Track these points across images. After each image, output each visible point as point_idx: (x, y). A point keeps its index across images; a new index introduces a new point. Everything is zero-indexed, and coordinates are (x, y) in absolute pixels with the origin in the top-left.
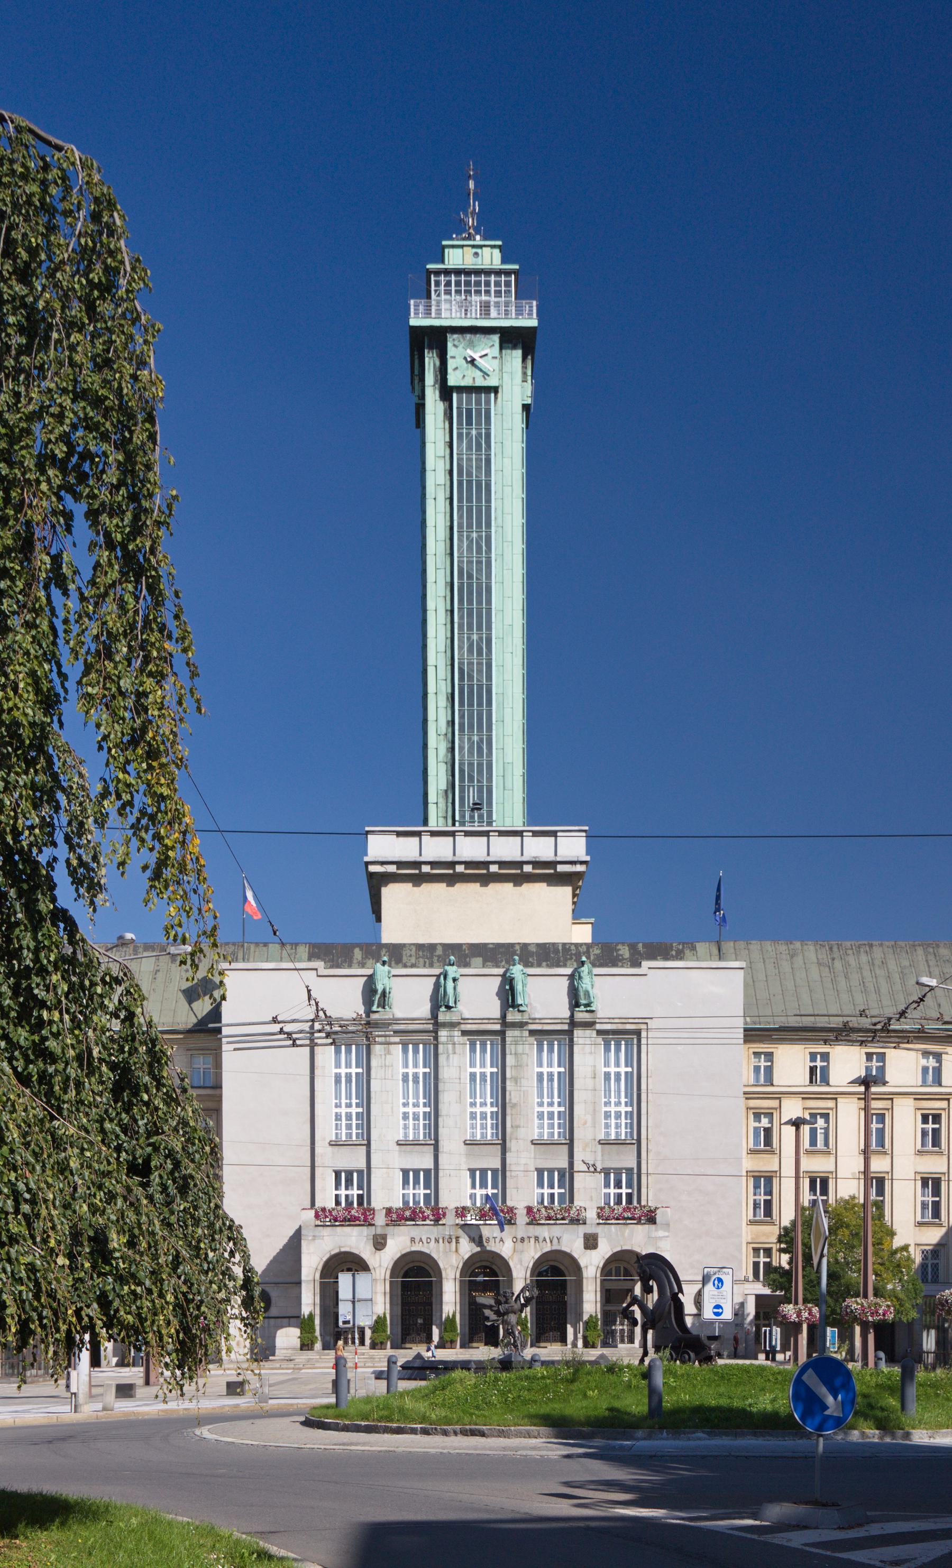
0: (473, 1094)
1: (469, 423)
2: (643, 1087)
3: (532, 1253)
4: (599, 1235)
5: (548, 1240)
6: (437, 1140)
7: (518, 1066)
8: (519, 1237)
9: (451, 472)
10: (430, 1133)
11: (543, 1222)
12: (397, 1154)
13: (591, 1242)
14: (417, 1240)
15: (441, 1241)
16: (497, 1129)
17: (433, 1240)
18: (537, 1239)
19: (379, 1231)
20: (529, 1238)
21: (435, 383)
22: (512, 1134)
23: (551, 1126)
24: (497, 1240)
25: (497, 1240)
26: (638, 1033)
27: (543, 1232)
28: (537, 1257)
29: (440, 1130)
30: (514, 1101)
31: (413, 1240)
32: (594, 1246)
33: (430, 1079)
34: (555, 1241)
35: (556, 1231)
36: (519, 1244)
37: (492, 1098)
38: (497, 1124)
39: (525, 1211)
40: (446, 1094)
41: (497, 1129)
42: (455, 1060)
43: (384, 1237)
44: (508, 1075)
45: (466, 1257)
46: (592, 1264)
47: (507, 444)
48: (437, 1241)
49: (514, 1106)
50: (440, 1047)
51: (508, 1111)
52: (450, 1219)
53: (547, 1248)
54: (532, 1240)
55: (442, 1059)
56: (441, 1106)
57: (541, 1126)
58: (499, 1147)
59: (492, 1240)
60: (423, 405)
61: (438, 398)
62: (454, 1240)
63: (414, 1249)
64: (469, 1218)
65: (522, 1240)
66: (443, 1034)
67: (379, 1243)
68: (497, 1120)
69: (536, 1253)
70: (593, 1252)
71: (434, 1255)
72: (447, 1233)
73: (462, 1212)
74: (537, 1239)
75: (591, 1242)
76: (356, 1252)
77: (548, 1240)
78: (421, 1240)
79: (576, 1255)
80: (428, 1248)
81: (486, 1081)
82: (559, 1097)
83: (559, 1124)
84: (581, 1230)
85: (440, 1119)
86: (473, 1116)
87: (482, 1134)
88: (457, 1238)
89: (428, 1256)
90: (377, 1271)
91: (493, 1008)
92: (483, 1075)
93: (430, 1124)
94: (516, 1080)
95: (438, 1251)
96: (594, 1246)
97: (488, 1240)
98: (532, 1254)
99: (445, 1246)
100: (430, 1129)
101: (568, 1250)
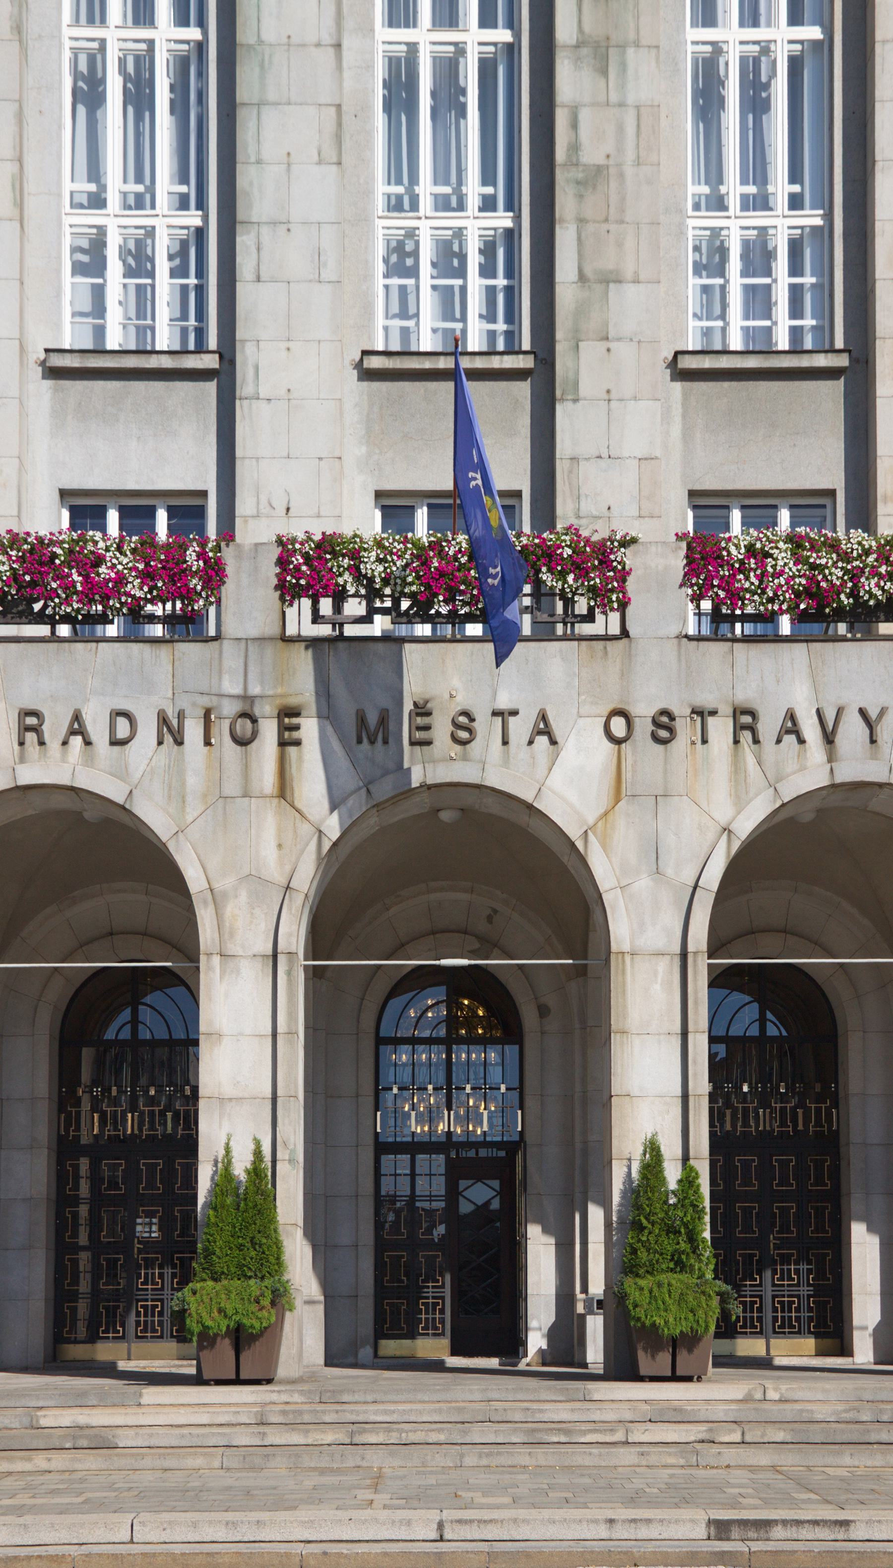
0: (402, 165)
3: (717, 806)
6: (227, 354)
8: (644, 710)
10: (200, 333)
15: (193, 731)
16: (511, 316)
18: (745, 720)
20: (701, 713)
22: (581, 311)
23: (759, 301)
24: (520, 728)
25: (520, 728)
29: (244, 292)
30: (591, 155)
33: (202, 74)
36: (644, 753)
37: (488, 178)
38: (511, 293)
39: (678, 563)
40: (270, 117)
41: (511, 316)
48: (170, 730)
49: (594, 177)
51: (565, 202)
52: (247, 601)
54: (720, 729)
56: (245, 176)
57: (714, 302)
58: (523, 390)
59: (487, 730)
62: (269, 730)
64: (354, 607)
68: (511, 271)
72: (231, 686)
73: (310, 569)
74: (745, 720)
78: (77, 727)
80: (121, 773)
81: (462, 111)
82: (795, 176)
83: (796, 292)
85: (244, 241)
86: (402, 259)
88: (288, 716)
92: (448, 69)
93: (200, 290)
95: (178, 795)
97: (464, 728)
98: (723, 812)
99: (217, 767)
100: (201, 315)
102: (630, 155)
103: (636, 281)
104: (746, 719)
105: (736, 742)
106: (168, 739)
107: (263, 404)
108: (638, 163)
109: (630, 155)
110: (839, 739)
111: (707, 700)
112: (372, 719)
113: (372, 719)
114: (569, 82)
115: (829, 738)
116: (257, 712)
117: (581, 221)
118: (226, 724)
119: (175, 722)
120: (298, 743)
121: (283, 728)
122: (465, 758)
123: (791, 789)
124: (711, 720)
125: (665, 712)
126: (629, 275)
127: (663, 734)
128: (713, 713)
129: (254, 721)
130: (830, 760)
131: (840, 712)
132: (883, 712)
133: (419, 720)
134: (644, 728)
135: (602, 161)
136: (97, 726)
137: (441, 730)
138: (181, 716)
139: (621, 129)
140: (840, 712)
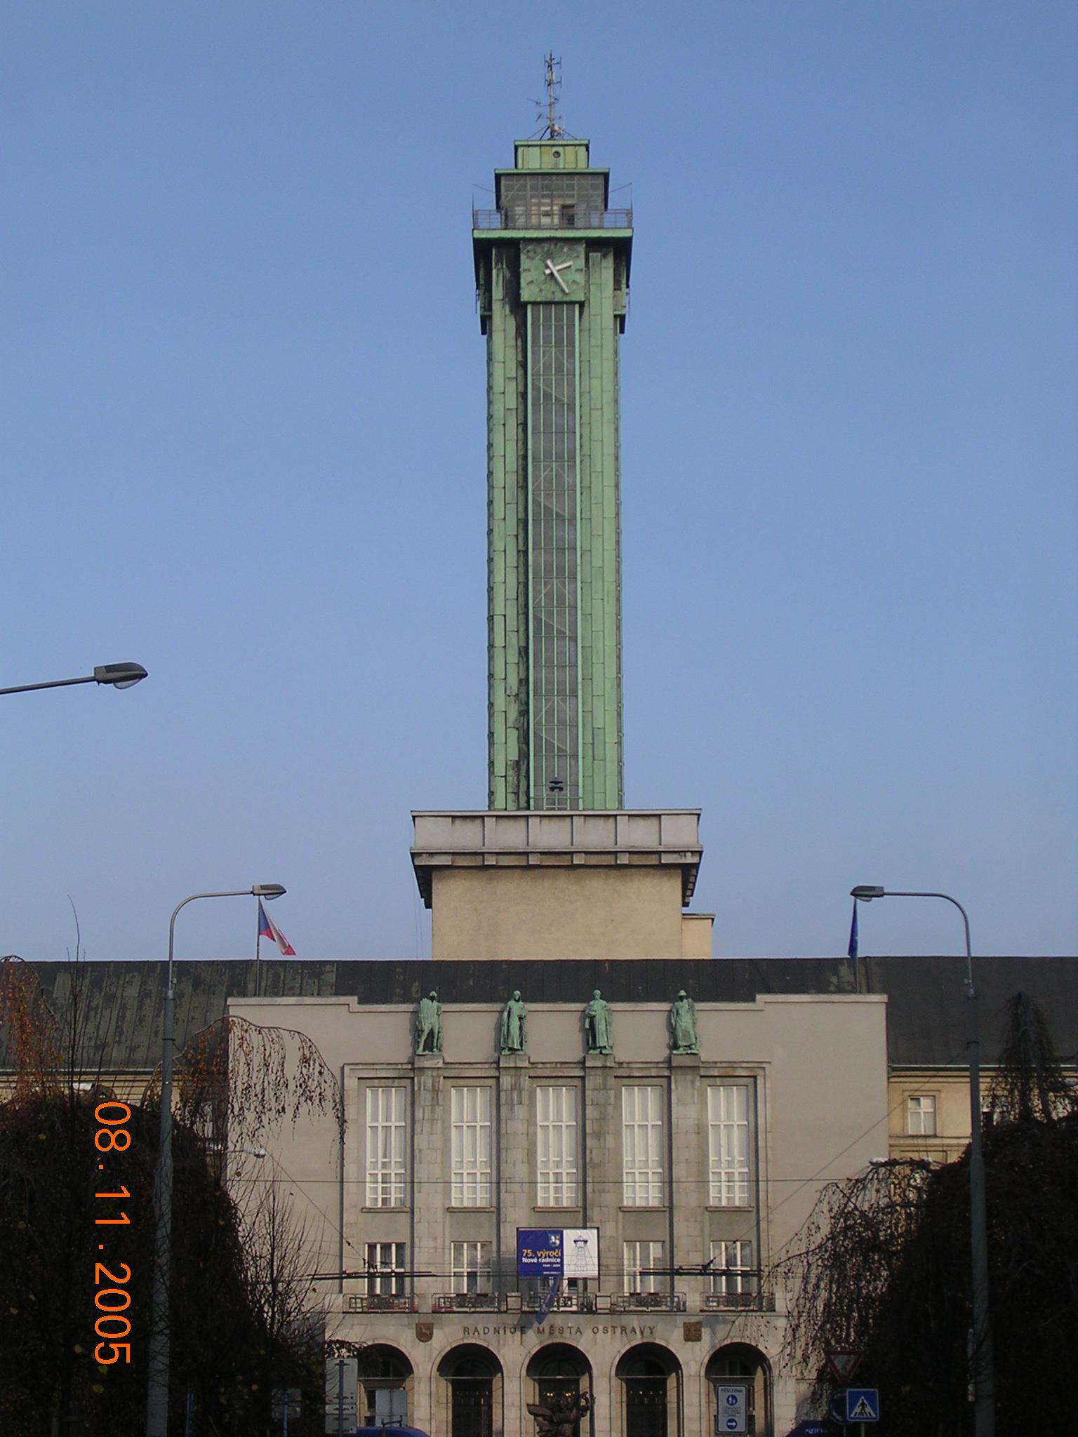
1: (547, 340)
2: (761, 1143)
6: (498, 1209)
7: (603, 1118)
9: (524, 395)
11: (632, 1308)
12: (447, 1225)
15: (502, 1332)
17: (492, 1330)
19: (424, 1319)
21: (506, 295)
24: (573, 1331)
25: (573, 1331)
26: (755, 1077)
27: (634, 1322)
28: (623, 1351)
30: (596, 1160)
31: (466, 1330)
32: (698, 1338)
34: (647, 1332)
35: (648, 1320)
42: (521, 1112)
43: (430, 1327)
44: (588, 1130)
47: (595, 362)
48: (497, 1331)
50: (503, 1095)
53: (637, 1340)
54: (618, 1331)
55: (503, 1110)
60: (490, 317)
61: (507, 312)
63: (466, 1341)
66: (506, 1081)
67: (424, 1334)
74: (624, 1329)
84: (680, 1320)
87: (557, 1199)
89: (487, 1349)
91: (572, 1049)
94: (599, 1135)
96: (698, 1338)
114: (590, 1142)
123: (634, 1343)
137: (557, 1331)
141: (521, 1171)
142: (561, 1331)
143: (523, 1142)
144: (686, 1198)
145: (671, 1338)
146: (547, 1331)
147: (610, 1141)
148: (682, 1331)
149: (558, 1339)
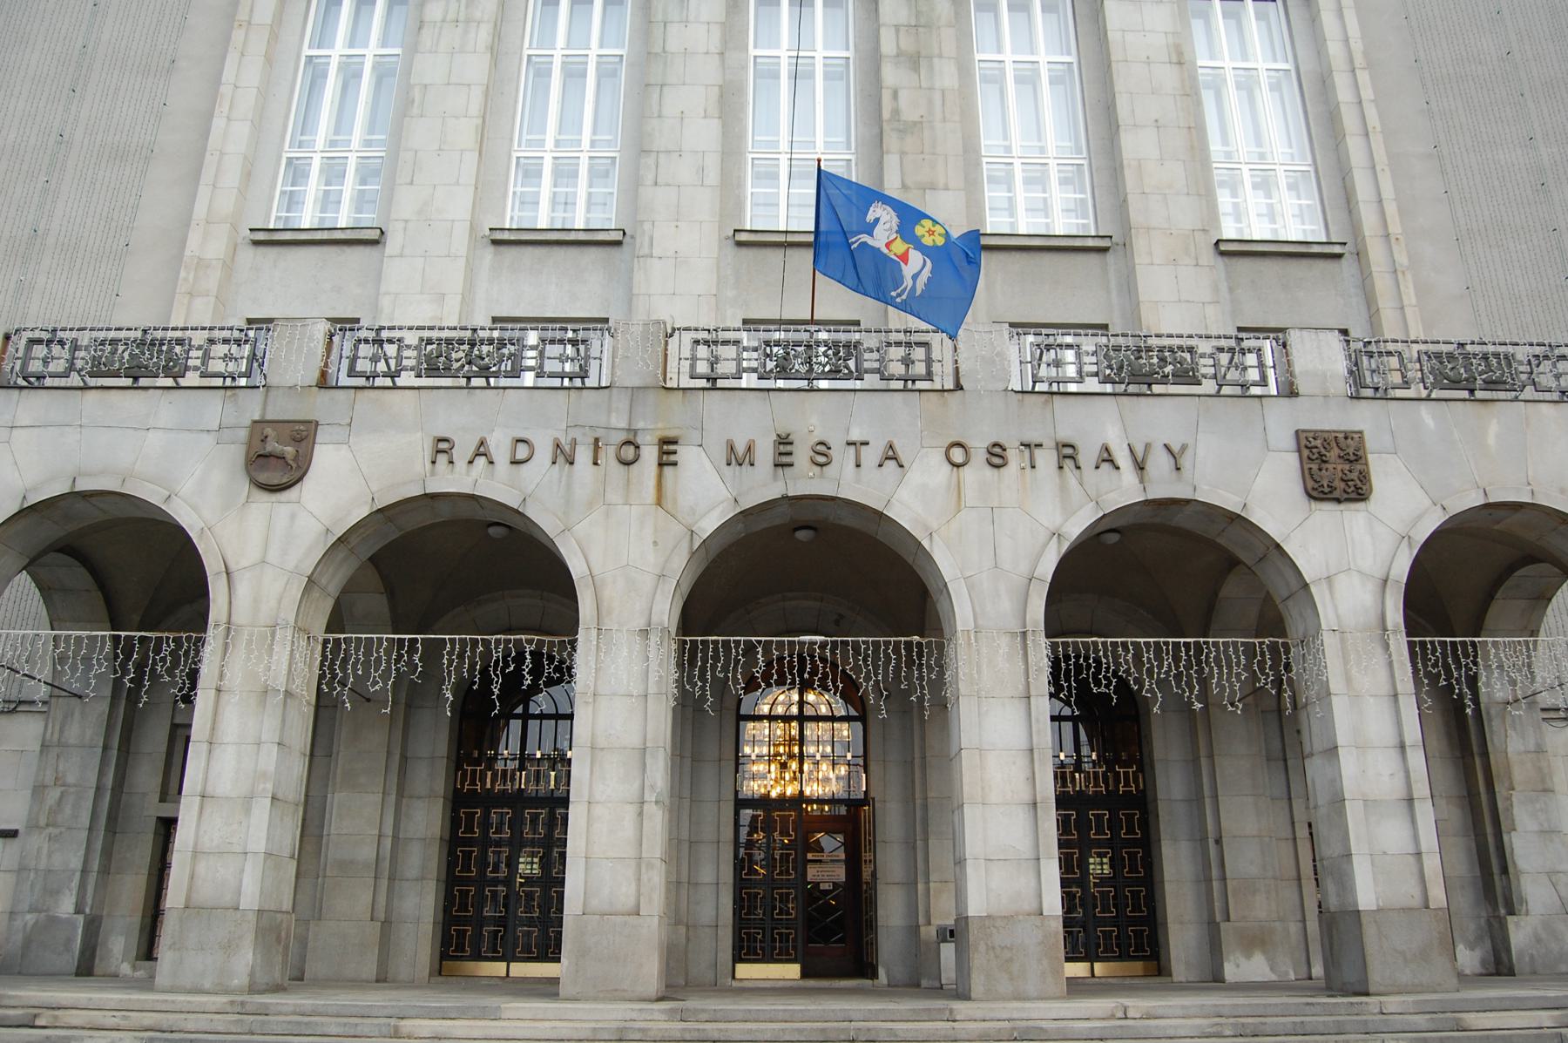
4: (1370, 443)
5: (1123, 459)
13: (1334, 472)
14: (462, 452)
15: (583, 455)
17: (544, 453)
18: (1067, 453)
24: (871, 456)
25: (871, 456)
30: (909, 114)
31: (442, 447)
35: (1161, 418)
43: (303, 435)
44: (888, 46)
45: (709, 524)
46: (1350, 566)
48: (564, 455)
51: (891, 141)
53: (1123, 490)
59: (843, 459)
62: (650, 454)
65: (997, 456)
67: (276, 461)
69: (1069, 512)
70: (1353, 517)
71: (545, 519)
74: (1067, 453)
75: (1334, 472)
76: (152, 494)
77: (1123, 459)
78: (481, 450)
79: (1271, 526)
88: (667, 445)
90: (243, 590)
94: (914, 61)
101: (1231, 503)
102: (938, 115)
103: (946, 189)
104: (1068, 451)
105: (1061, 468)
106: (561, 459)
107: (655, 261)
108: (944, 120)
109: (938, 115)
110: (1149, 466)
111: (1033, 437)
112: (740, 449)
113: (740, 449)
114: (890, 75)
115: (1140, 467)
116: (639, 441)
117: (903, 154)
118: (611, 451)
119: (567, 448)
120: (675, 464)
121: (662, 453)
122: (822, 476)
124: (1037, 452)
125: (995, 445)
126: (941, 185)
127: (996, 461)
128: (1039, 445)
129: (637, 447)
130: (1142, 481)
131: (1148, 447)
132: (1184, 448)
133: (782, 448)
134: (979, 456)
135: (917, 119)
136: (501, 453)
137: (801, 455)
138: (574, 443)
139: (930, 102)
140: (1148, 447)
141: (703, 134)
142: (822, 454)
143: (708, 71)
144: (1160, 214)
145: (1270, 497)
146: (765, 453)
147: (947, 76)
148: (1293, 460)
149: (805, 482)
